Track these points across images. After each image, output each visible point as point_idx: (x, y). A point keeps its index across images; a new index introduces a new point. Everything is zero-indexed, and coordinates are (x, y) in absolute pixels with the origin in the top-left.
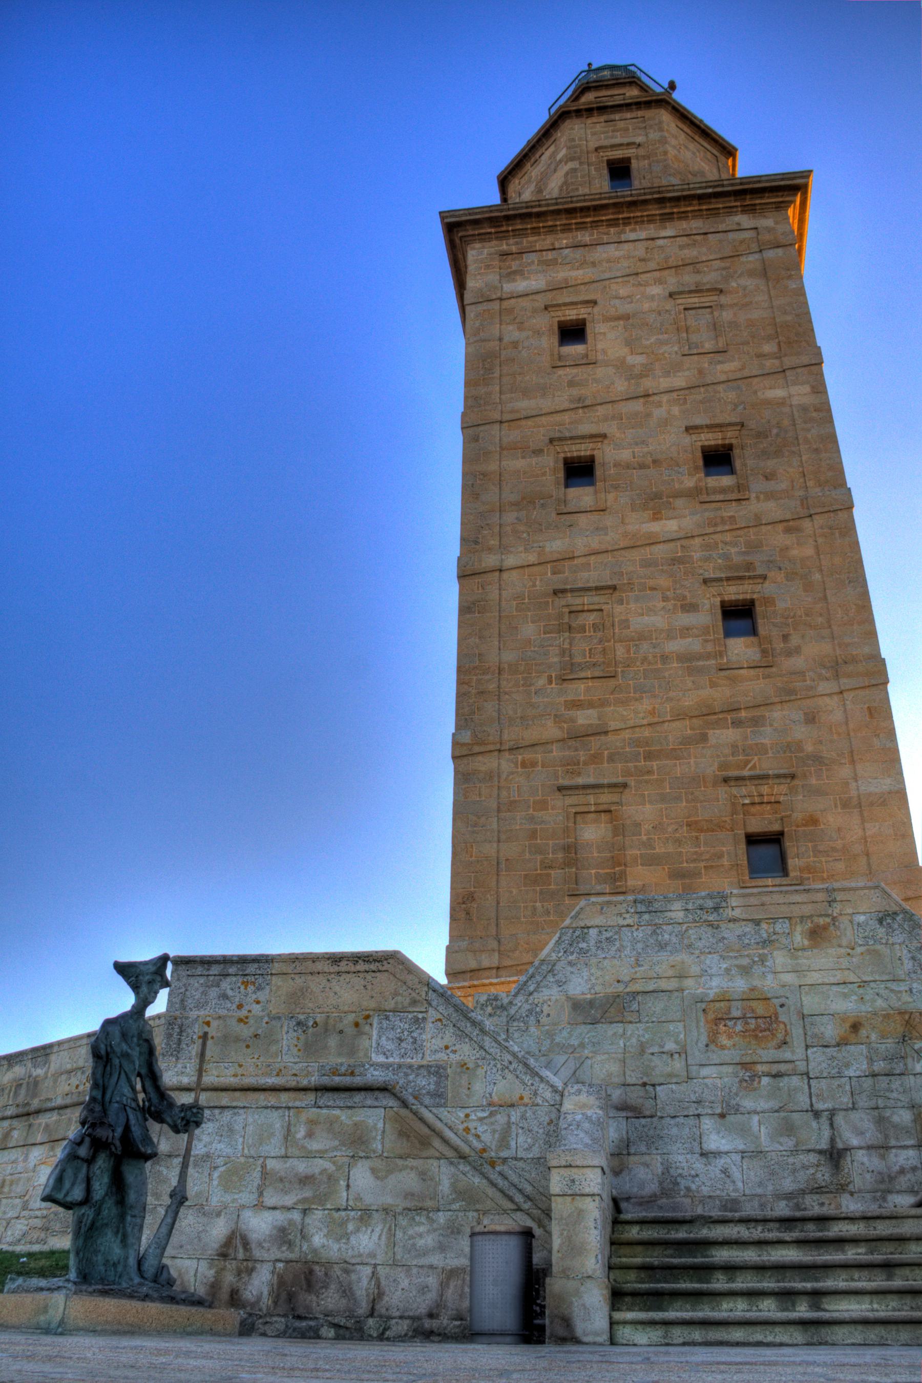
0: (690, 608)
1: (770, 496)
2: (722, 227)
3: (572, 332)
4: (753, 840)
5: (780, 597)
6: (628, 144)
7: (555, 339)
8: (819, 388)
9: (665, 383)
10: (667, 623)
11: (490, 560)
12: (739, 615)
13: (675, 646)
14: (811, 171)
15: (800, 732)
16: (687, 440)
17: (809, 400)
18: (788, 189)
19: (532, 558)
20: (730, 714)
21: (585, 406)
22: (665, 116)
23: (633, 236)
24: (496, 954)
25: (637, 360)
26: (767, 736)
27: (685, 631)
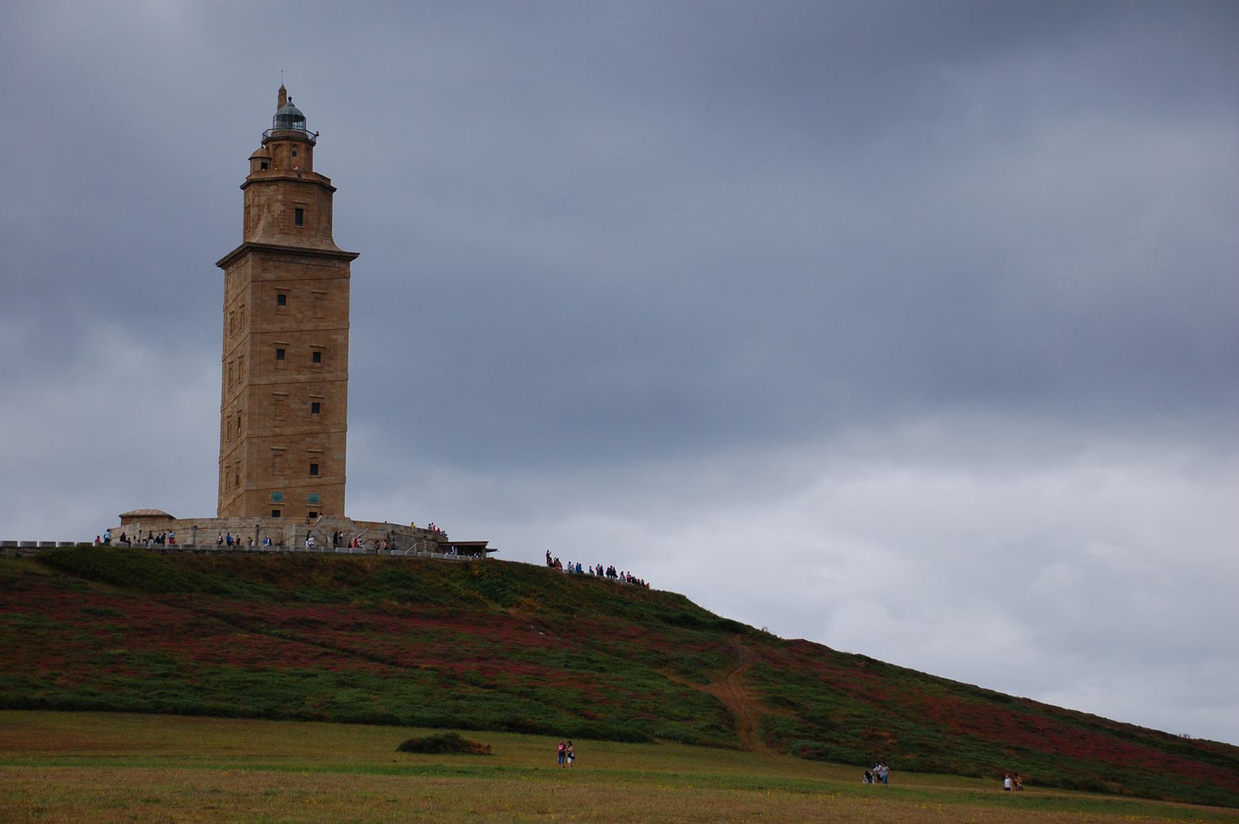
0: (305, 403)
3: (282, 299)
8: (347, 338)
12: (316, 408)
13: (301, 413)
25: (299, 316)
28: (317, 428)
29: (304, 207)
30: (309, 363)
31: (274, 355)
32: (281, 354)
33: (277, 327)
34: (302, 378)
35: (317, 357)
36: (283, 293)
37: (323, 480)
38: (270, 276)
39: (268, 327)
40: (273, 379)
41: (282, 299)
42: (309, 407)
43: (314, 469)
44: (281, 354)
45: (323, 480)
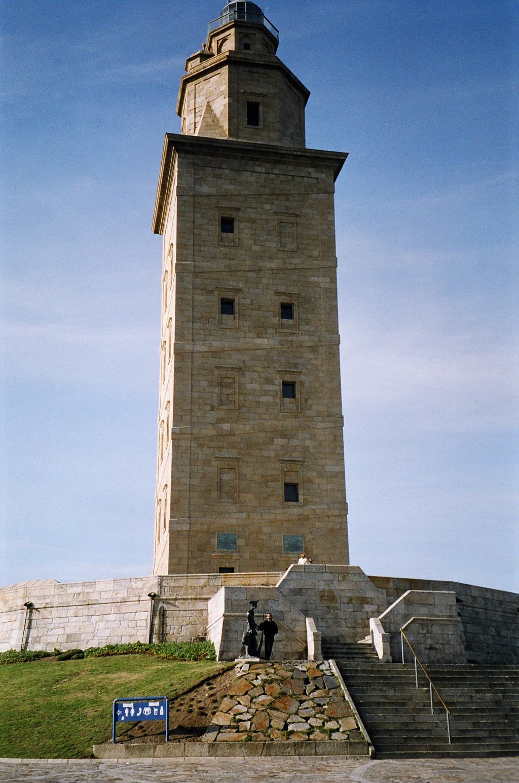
1: (307, 333)
2: (303, 174)
3: (227, 225)
4: (286, 485)
5: (305, 380)
6: (260, 94)
7: (219, 228)
8: (334, 281)
9: (269, 265)
10: (261, 388)
11: (189, 347)
12: (289, 389)
14: (346, 155)
15: (308, 443)
16: (277, 298)
17: (328, 286)
18: (333, 162)
19: (205, 349)
20: (283, 435)
21: (231, 271)
22: (278, 75)
23: (258, 169)
24: (189, 525)
25: (256, 248)
26: (295, 442)
27: (266, 393)
28: (290, 423)
29: (260, 100)
30: (276, 320)
31: (217, 307)
32: (227, 306)
33: (220, 265)
34: (264, 342)
35: (287, 310)
36: (227, 214)
37: (308, 510)
38: (205, 189)
39: (205, 265)
40: (216, 344)
41: (227, 225)
42: (277, 387)
43: (291, 492)
44: (227, 306)
45: (308, 510)
